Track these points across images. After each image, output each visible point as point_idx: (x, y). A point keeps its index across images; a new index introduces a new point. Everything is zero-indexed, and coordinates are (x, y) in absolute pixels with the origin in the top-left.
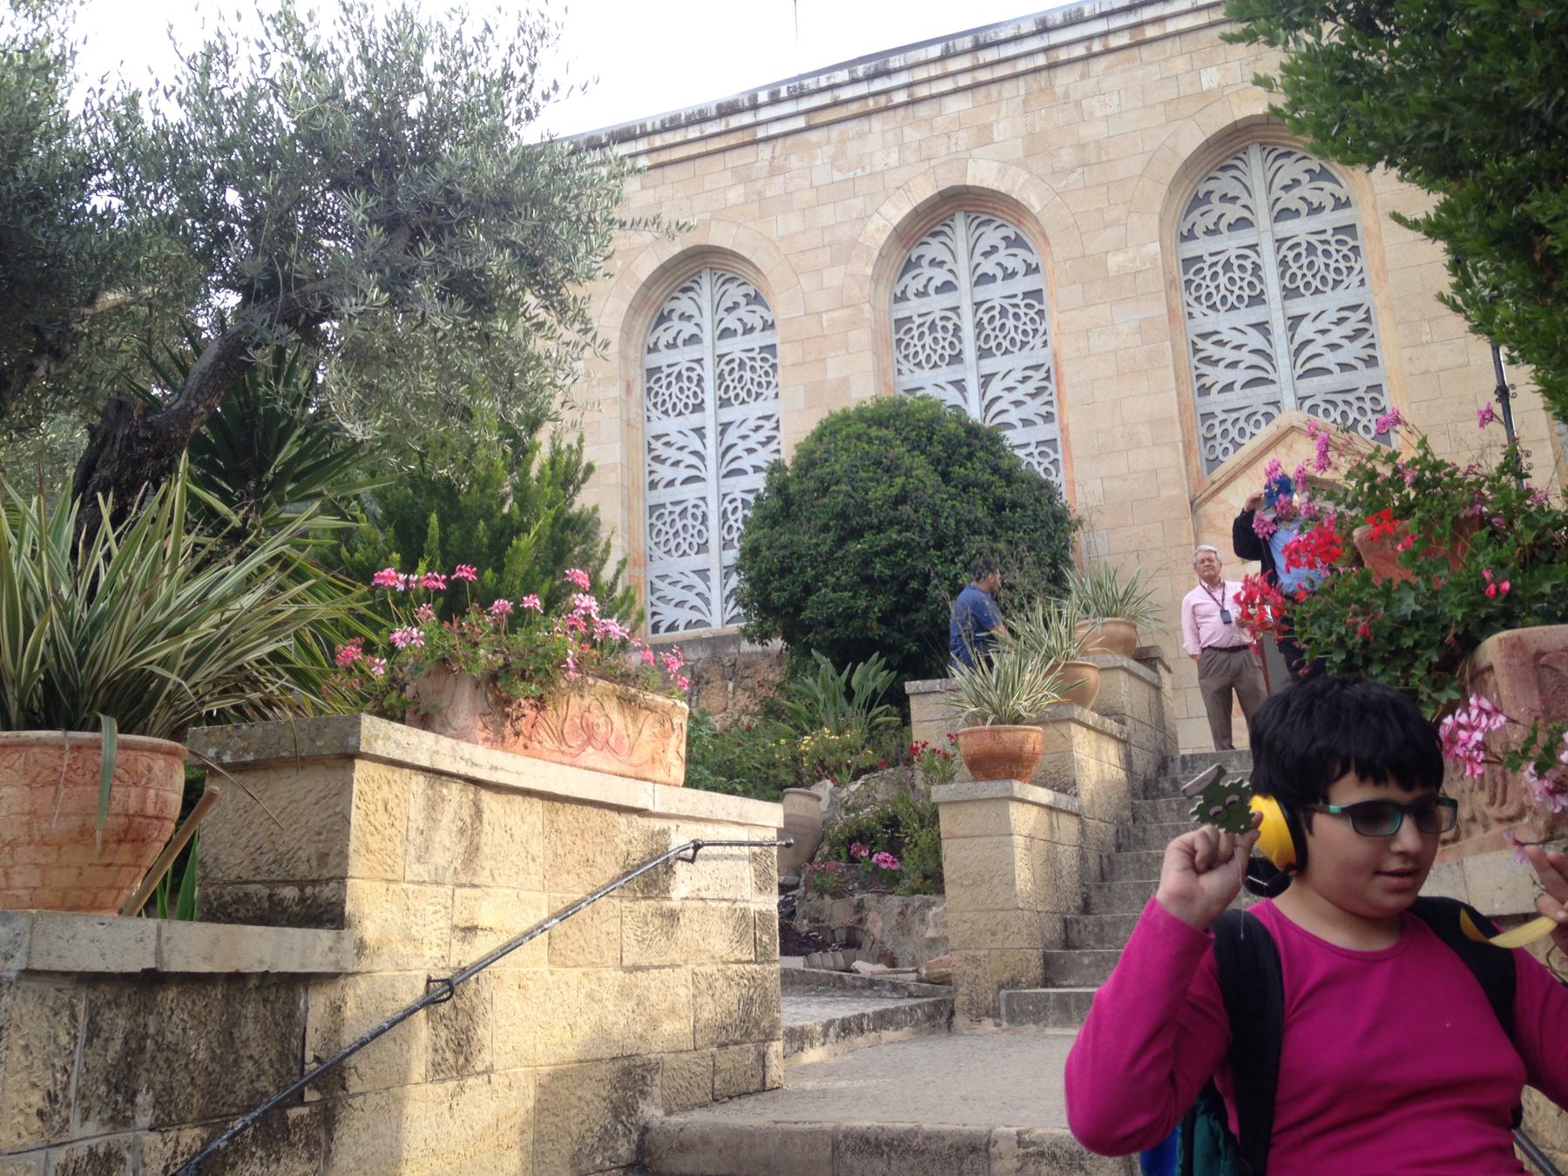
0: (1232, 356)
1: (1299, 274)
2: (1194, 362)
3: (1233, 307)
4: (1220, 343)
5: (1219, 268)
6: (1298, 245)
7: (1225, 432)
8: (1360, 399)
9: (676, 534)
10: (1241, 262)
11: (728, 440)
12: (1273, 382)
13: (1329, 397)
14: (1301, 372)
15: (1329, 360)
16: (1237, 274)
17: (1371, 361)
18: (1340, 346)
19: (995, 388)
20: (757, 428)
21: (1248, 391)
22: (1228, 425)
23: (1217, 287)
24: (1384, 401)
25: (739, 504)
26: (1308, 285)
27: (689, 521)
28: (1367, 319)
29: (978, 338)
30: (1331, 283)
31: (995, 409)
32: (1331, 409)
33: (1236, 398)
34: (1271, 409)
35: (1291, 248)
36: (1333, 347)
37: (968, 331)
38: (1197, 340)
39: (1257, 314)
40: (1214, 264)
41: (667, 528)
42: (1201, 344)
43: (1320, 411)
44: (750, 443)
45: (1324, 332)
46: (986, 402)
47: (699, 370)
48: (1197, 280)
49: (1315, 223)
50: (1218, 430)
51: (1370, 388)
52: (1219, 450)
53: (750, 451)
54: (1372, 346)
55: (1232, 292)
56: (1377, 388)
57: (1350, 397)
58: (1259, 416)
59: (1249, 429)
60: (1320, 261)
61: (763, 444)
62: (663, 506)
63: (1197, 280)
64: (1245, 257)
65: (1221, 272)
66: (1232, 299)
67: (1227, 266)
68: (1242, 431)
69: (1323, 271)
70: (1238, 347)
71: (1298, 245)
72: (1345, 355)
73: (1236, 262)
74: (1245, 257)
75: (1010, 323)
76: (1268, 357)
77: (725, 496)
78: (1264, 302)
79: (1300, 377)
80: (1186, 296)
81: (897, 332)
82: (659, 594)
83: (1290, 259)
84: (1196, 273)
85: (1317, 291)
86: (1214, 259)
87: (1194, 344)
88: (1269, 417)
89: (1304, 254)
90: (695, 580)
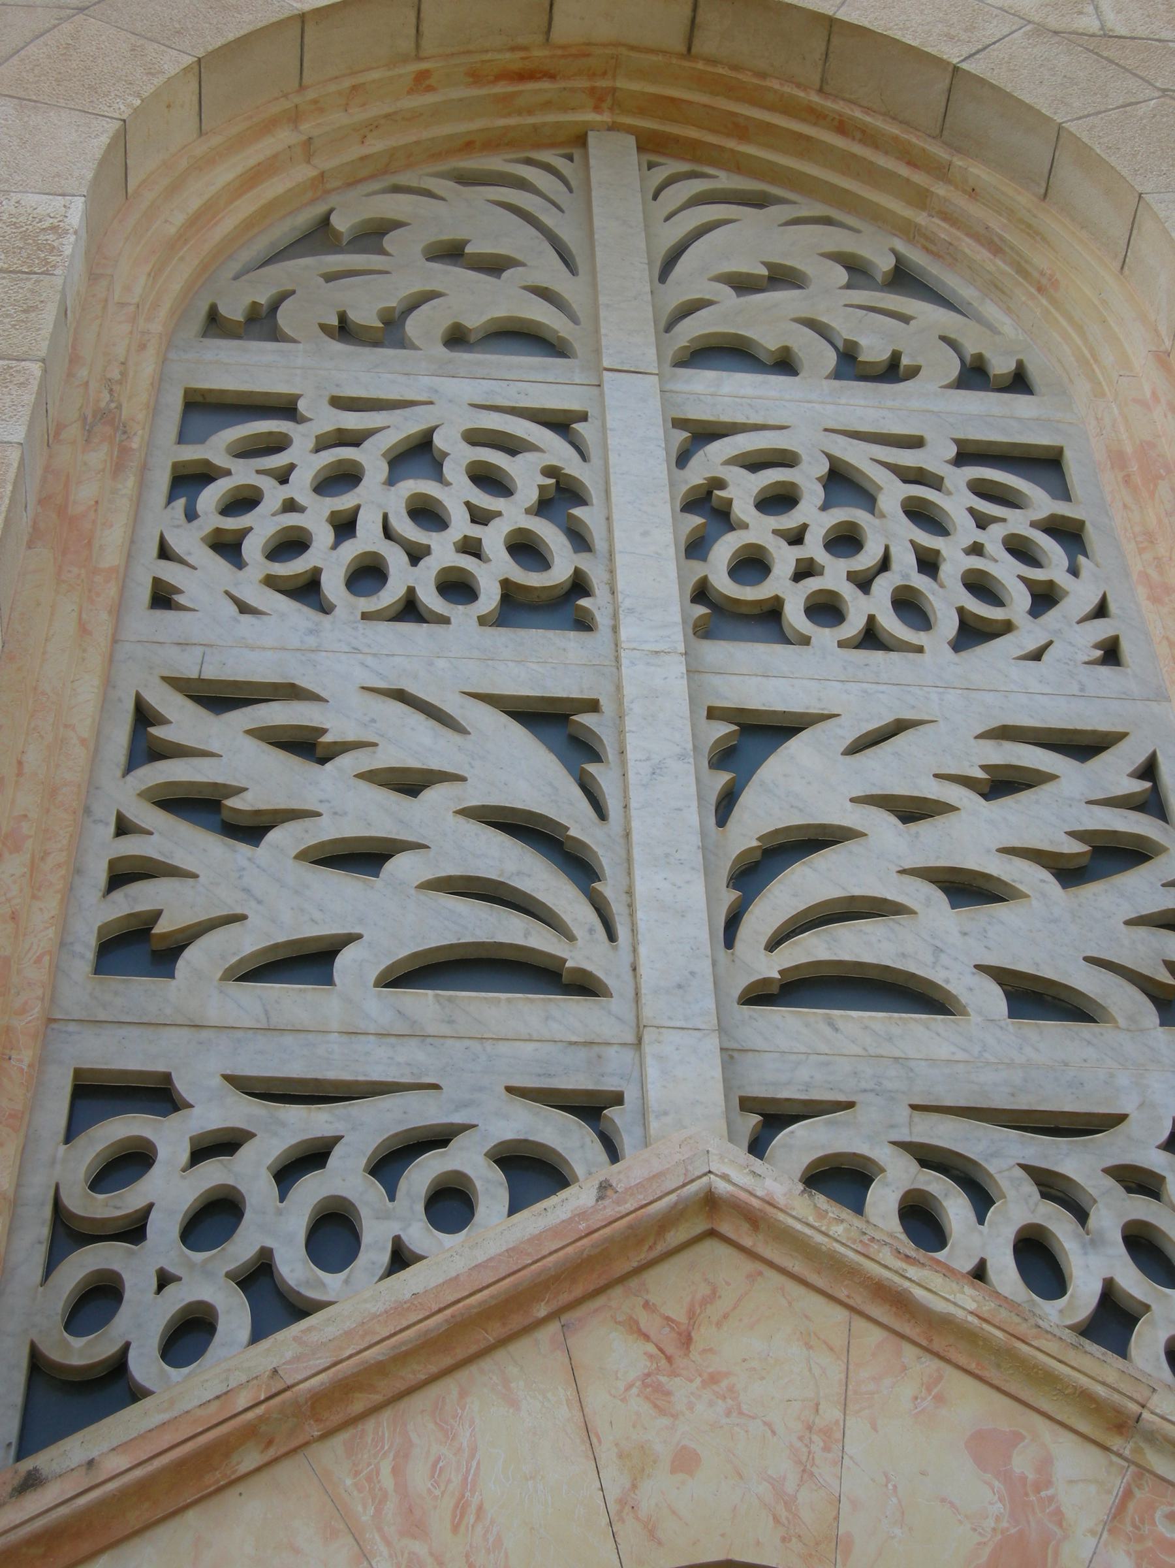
6: (786, 459)
14: (771, 967)
35: (755, 463)
48: (244, 474)
64: (511, 446)
74: (511, 446)
78: (584, 624)
86: (352, 421)
87: (144, 716)
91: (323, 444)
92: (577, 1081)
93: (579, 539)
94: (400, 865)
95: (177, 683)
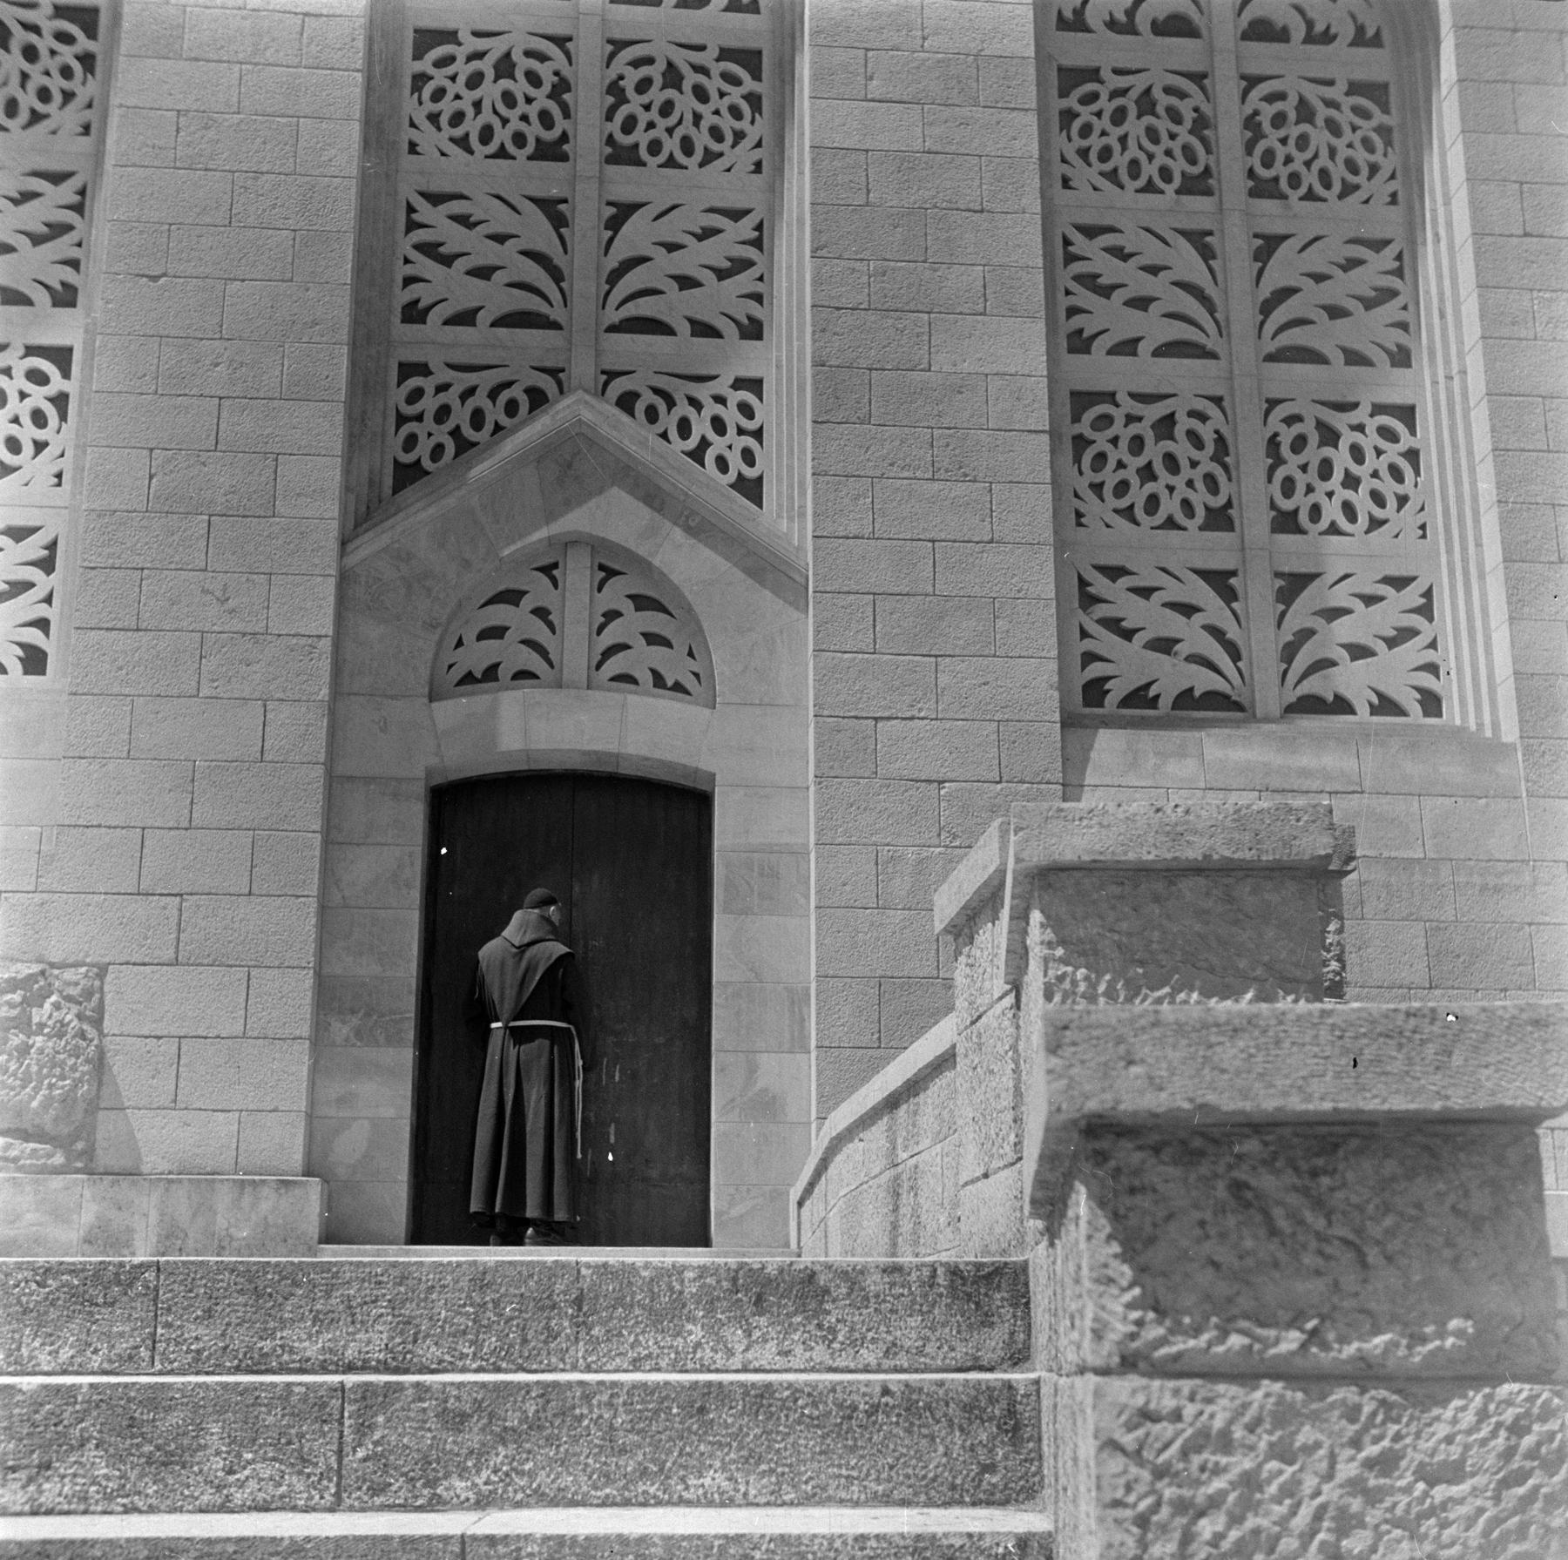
0: (489, 253)
1: (1281, 152)
2: (405, 246)
3: (502, 153)
4: (1120, 254)
5: (1129, 102)
7: (443, 413)
8: (720, 400)
9: (1147, 473)
10: (1174, 101)
11: (1277, 276)
12: (556, 326)
13: (663, 382)
15: (673, 306)
16: (520, 87)
17: (753, 330)
18: (696, 284)
19: (637, 235)
20: (707, 233)
21: (502, 332)
22: (451, 397)
23: (1123, 140)
24: (765, 413)
25: (1308, 428)
26: (654, 148)
27: (1182, 449)
28: (757, 243)
29: (609, 117)
30: (699, 154)
31: (634, 280)
32: (662, 407)
33: (471, 342)
34: (546, 383)
35: (636, 63)
36: (686, 282)
37: (1229, 133)
38: (420, 203)
39: (549, 179)
40: (479, 55)
41: (1122, 452)
42: (425, 212)
43: (640, 407)
44: (685, 263)
45: (672, 247)
46: (612, 262)
47: (1197, 98)
49: (1322, 60)
50: (429, 404)
51: (739, 384)
52: (423, 450)
53: (686, 282)
54: (758, 298)
55: (505, 121)
56: (755, 385)
57: (703, 392)
58: (516, 392)
59: (495, 413)
60: (685, 103)
61: (722, 275)
62: (1110, 397)
63: (440, 78)
64: (542, 58)
65: (1132, 112)
66: (502, 136)
67: (1146, 104)
68: (477, 419)
69: (1323, 161)
70: (500, 239)
71: (650, 61)
72: (701, 304)
73: (1163, 101)
74: (542, 58)
75: (685, 103)
76: (557, 275)
77: (1273, 403)
78: (564, 158)
79: (612, 329)
80: (1059, 140)
81: (418, 56)
82: (1101, 611)
83: (628, 86)
84: (442, 63)
85: (671, 163)
87: (411, 209)
88: (538, 399)
89: (658, 81)
90: (1203, 594)
91: (470, 59)
92: (549, 363)
93: (567, 114)
94: (497, 275)
95: (422, 194)
